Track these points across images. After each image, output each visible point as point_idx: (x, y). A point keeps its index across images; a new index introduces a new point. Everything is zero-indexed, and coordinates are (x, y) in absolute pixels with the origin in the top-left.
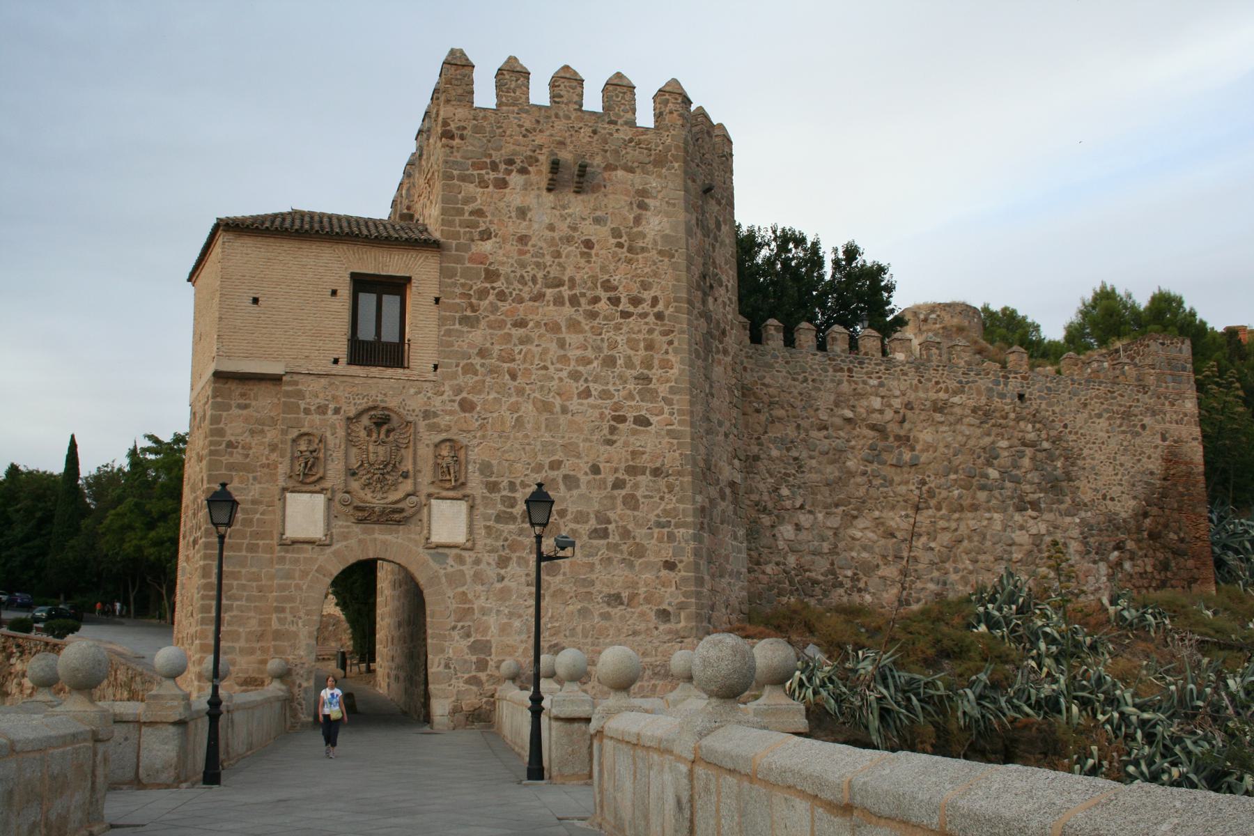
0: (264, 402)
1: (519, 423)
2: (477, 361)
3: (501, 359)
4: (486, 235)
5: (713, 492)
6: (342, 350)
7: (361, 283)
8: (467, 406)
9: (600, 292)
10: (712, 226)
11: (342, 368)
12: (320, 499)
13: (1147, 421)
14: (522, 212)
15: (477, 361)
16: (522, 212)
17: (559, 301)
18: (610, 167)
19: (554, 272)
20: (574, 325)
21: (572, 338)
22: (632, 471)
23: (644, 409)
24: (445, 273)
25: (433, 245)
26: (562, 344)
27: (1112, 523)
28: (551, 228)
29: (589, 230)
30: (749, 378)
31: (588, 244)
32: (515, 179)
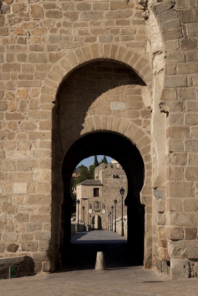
0: (87, 201)
1: (110, 202)
2: (106, 196)
3: (108, 195)
4: (107, 183)
6: (93, 196)
8: (105, 200)
9: (118, 188)
12: (92, 210)
14: (110, 180)
15: (106, 196)
16: (110, 180)
20: (116, 192)
25: (102, 185)
26: (114, 194)
28: (113, 182)
31: (117, 183)
32: (109, 177)
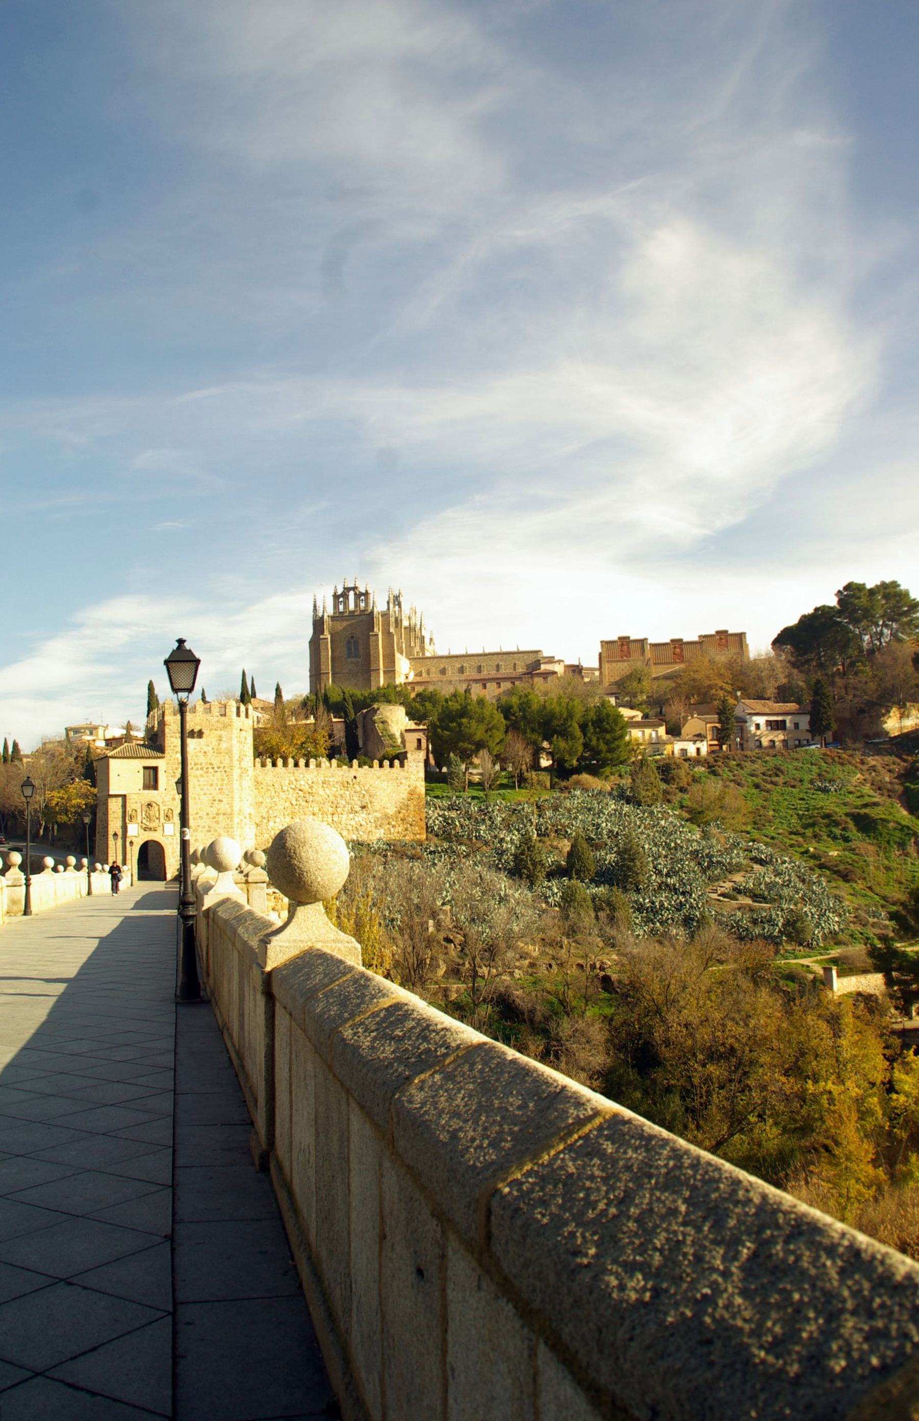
5: (242, 817)
7: (145, 768)
10: (243, 740)
11: (142, 791)
13: (404, 781)
17: (197, 769)
18: (211, 730)
19: (196, 761)
20: (202, 776)
21: (201, 779)
22: (217, 814)
23: (221, 797)
24: (168, 764)
27: (386, 816)
29: (206, 749)
30: (259, 779)
